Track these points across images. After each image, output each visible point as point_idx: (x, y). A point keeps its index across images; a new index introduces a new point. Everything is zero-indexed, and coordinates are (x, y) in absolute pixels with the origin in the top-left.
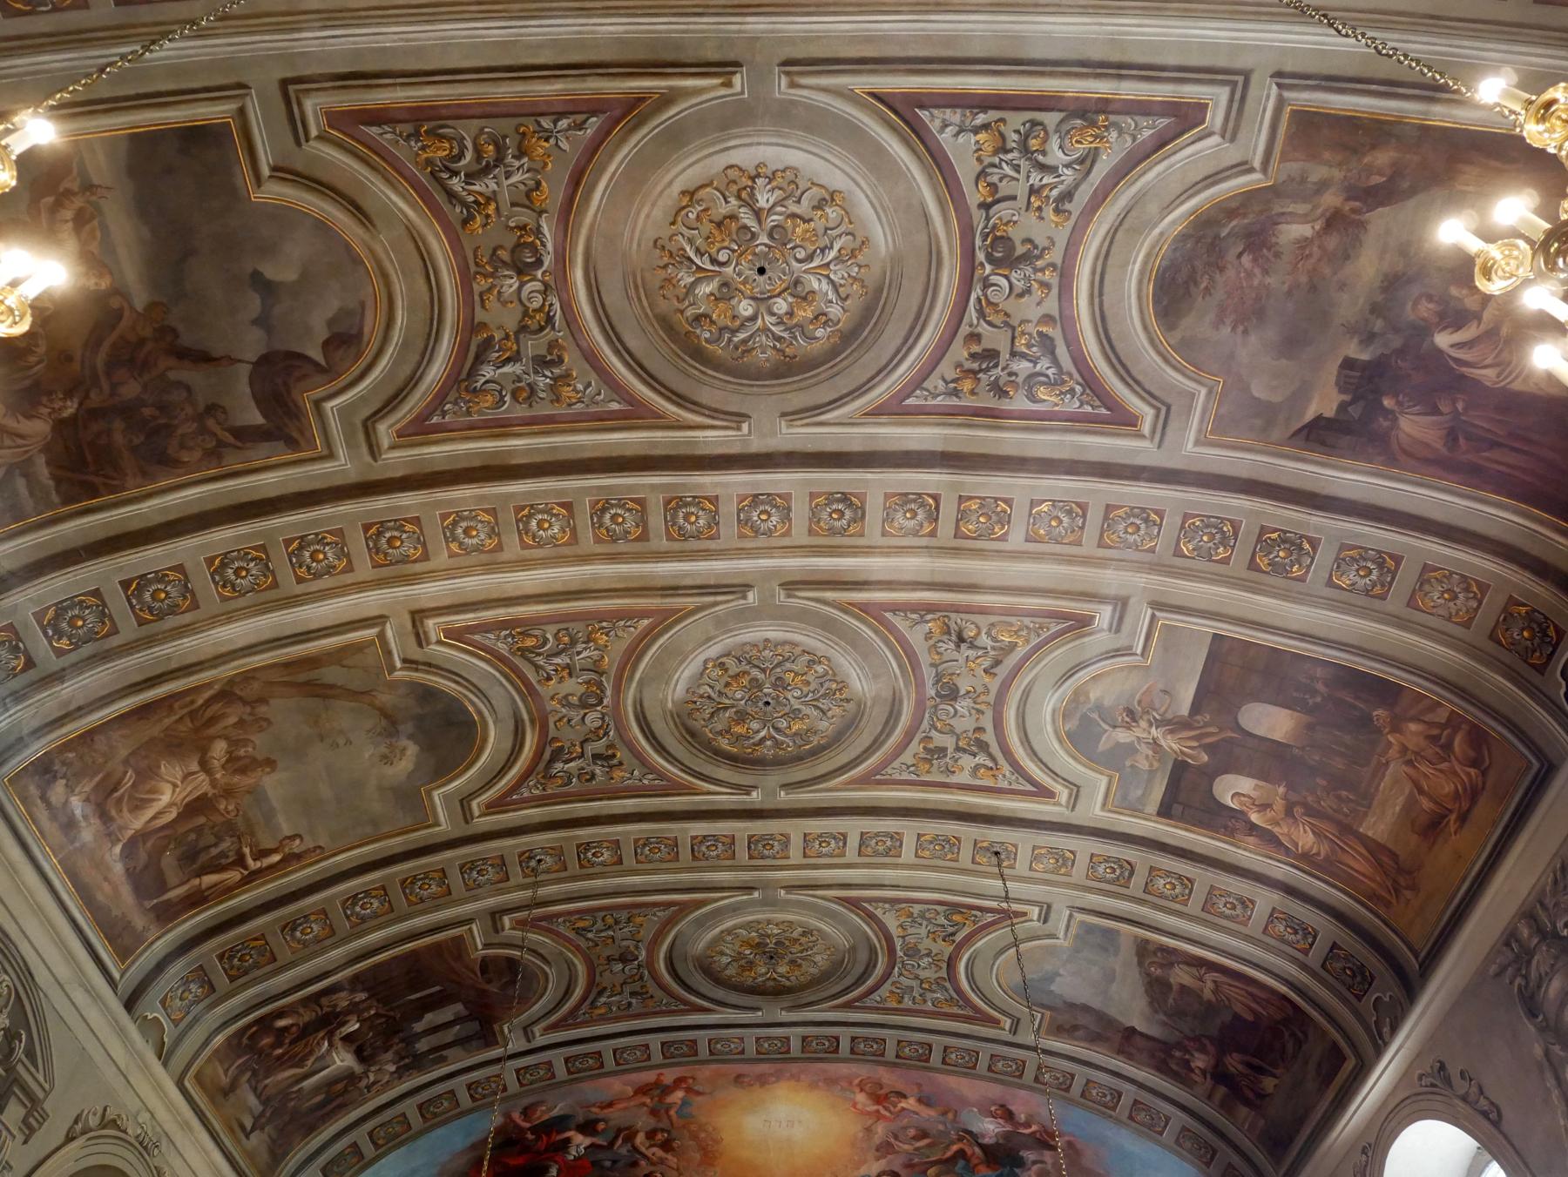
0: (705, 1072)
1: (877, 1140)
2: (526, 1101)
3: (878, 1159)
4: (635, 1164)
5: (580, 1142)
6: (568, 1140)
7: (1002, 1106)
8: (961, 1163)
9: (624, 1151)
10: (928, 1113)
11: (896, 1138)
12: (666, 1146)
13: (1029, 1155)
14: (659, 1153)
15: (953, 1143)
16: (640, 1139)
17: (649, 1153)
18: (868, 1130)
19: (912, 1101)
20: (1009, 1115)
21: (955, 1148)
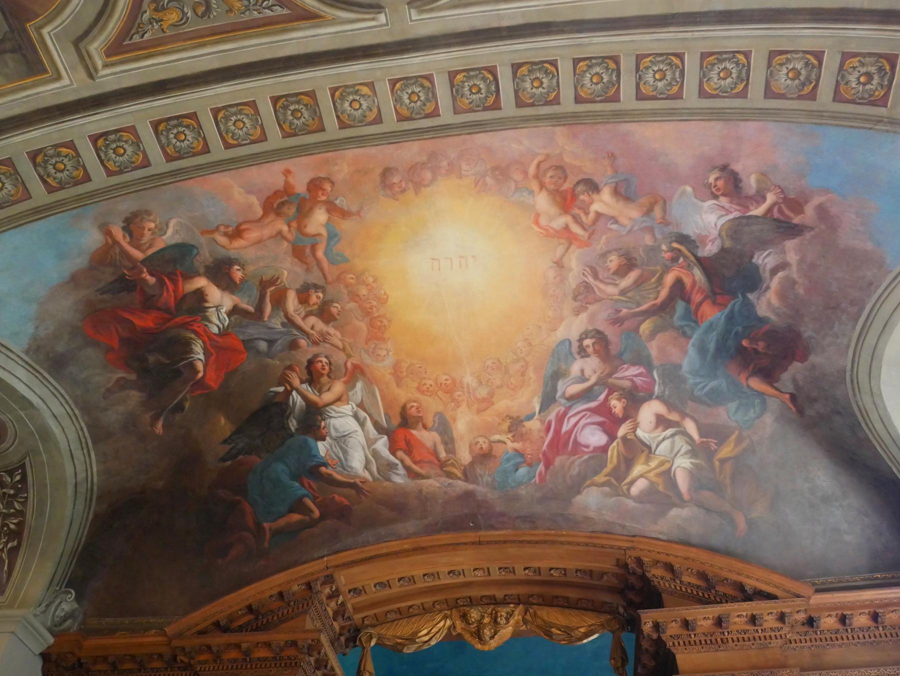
0: (342, 166)
1: (573, 281)
2: (127, 206)
3: (577, 312)
4: (294, 345)
5: (220, 301)
6: (200, 295)
7: (724, 168)
8: (680, 306)
9: (277, 323)
10: (630, 214)
11: (596, 276)
12: (324, 313)
13: (765, 260)
14: (320, 325)
15: (666, 270)
16: (292, 302)
17: (306, 325)
18: (559, 264)
19: (606, 195)
20: (732, 185)
21: (669, 279)
